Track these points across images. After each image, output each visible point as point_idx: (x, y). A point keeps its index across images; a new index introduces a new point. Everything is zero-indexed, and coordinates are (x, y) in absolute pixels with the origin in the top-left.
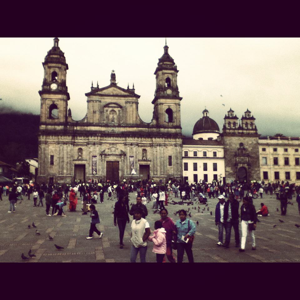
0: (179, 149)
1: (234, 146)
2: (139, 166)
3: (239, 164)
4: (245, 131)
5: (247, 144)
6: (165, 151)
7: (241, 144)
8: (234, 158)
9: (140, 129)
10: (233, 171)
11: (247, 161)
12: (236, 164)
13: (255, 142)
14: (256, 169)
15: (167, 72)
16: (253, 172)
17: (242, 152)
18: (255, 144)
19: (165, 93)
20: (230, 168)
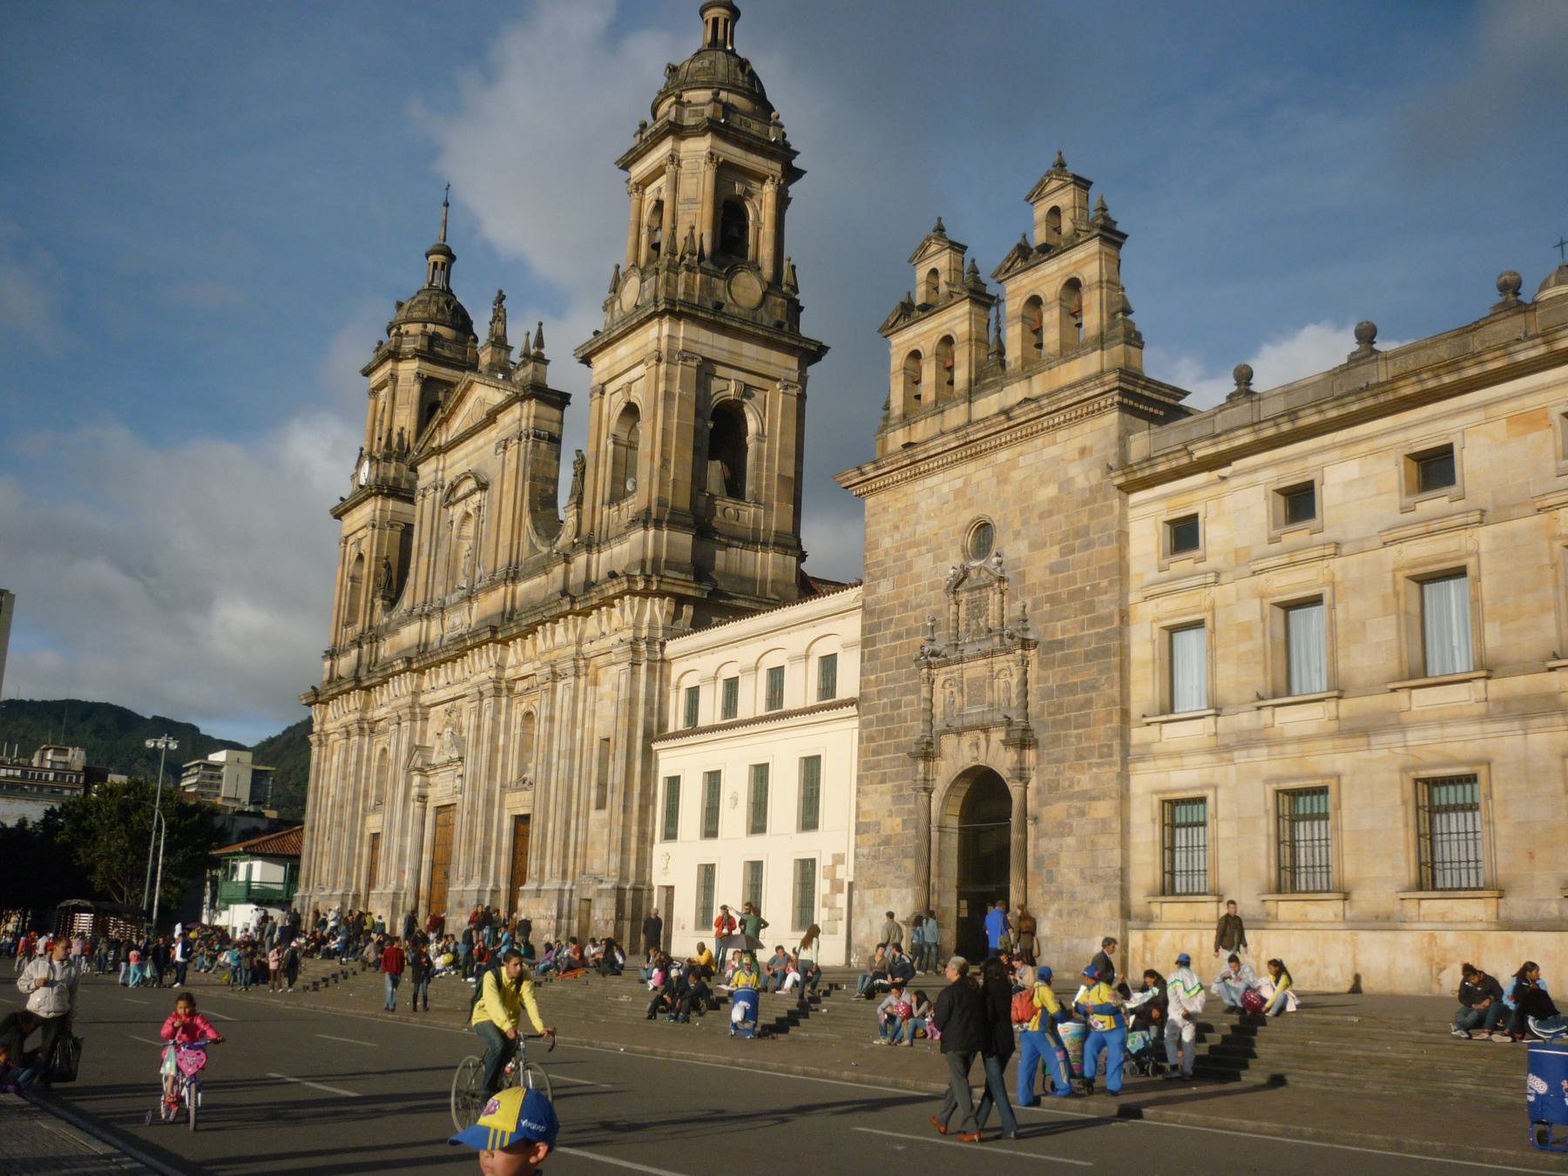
0: (623, 679)
1: (923, 563)
2: (507, 824)
3: (948, 743)
4: (1014, 393)
5: (1017, 525)
6: (580, 705)
7: (983, 533)
8: (917, 691)
9: (523, 587)
10: (904, 822)
11: (1015, 702)
12: (927, 752)
13: (1083, 476)
14: (1084, 781)
15: (646, 173)
16: (1056, 811)
17: (977, 609)
18: (1095, 492)
19: (616, 314)
20: (888, 785)
